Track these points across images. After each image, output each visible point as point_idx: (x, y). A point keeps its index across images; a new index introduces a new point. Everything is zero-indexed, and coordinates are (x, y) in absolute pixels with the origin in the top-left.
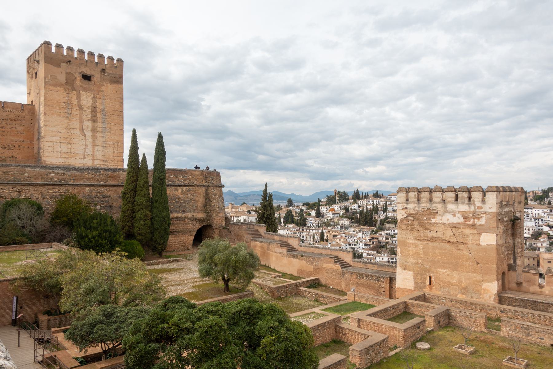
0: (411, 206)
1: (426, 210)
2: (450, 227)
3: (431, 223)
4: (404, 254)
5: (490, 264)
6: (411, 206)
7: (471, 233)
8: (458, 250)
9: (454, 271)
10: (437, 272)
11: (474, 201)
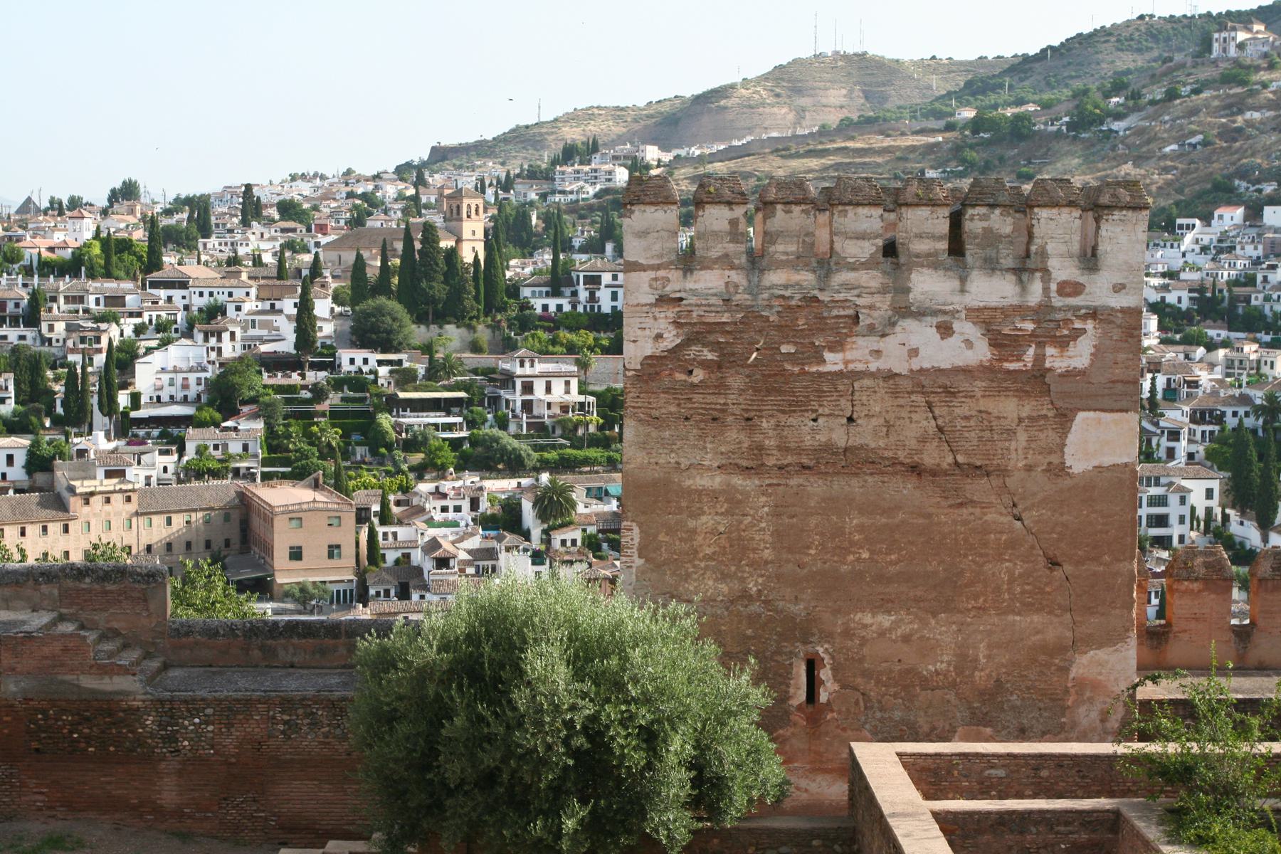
0: (709, 281)
1: (793, 303)
2: (921, 389)
3: (821, 375)
4: (665, 555)
5: (1107, 558)
6: (709, 281)
7: (1024, 415)
8: (961, 505)
9: (934, 615)
10: (848, 633)
11: (1043, 254)
